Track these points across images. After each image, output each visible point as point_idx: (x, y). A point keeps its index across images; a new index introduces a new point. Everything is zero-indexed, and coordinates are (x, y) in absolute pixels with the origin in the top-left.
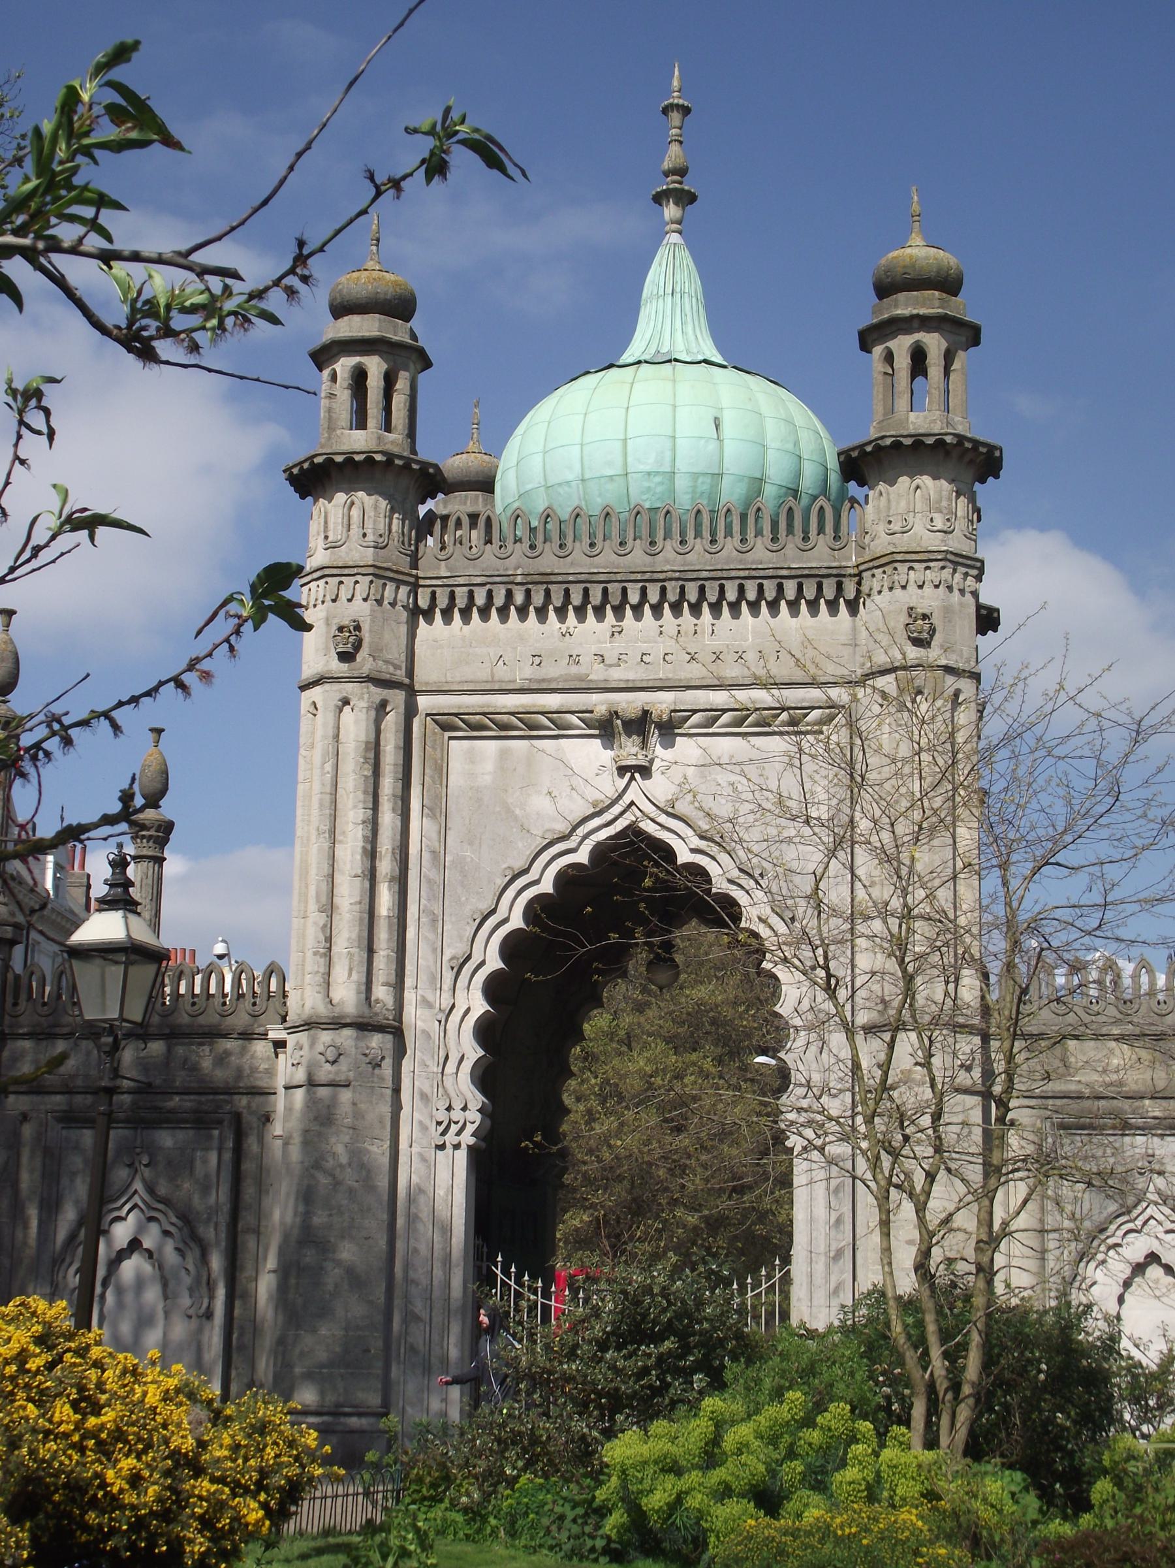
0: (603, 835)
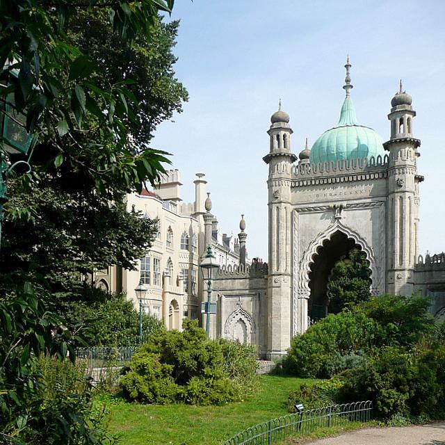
0: (332, 232)
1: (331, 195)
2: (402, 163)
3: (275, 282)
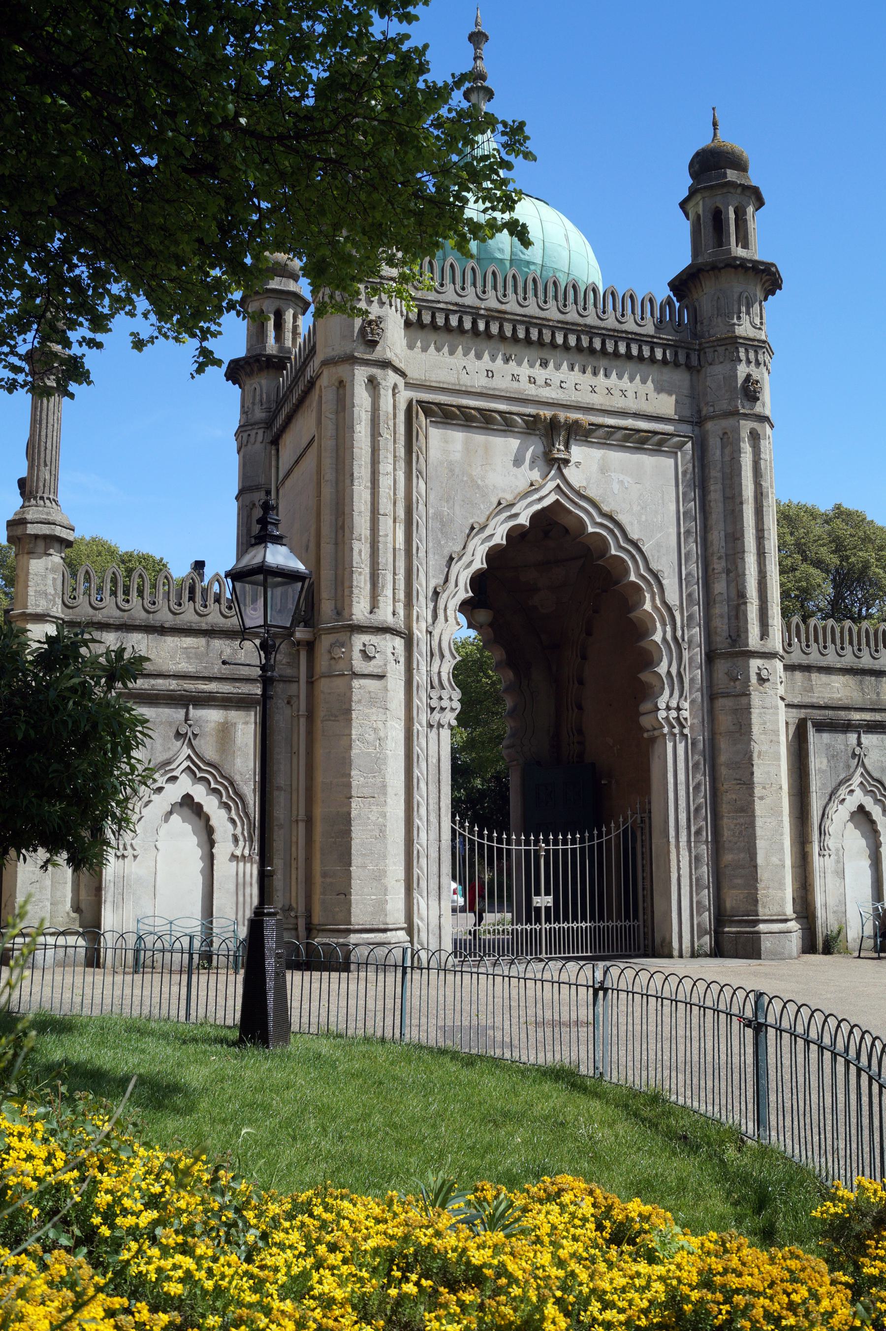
0: (538, 507)
1: (532, 380)
2: (751, 333)
3: (366, 657)
